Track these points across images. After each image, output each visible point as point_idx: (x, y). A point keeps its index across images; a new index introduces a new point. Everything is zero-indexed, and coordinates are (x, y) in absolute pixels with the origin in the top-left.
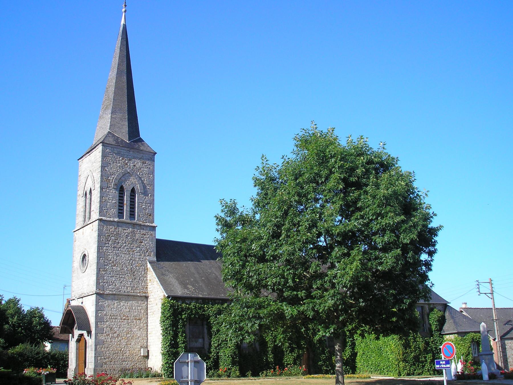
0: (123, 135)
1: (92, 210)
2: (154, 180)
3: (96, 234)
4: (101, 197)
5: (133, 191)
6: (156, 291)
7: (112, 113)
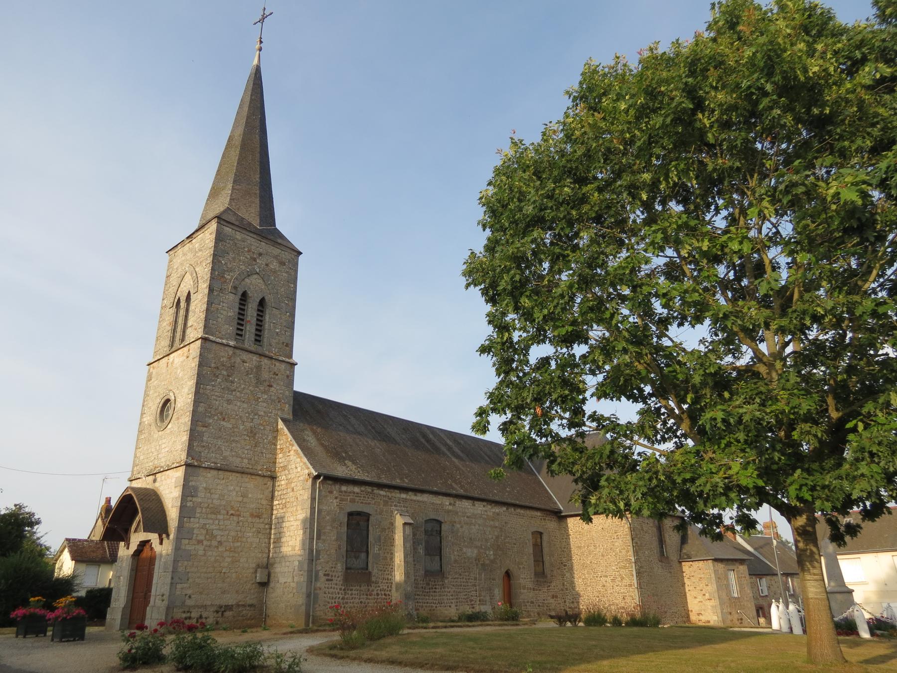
0: (252, 216)
1: (190, 323)
2: (295, 292)
3: (194, 364)
4: (210, 303)
5: (262, 303)
6: (293, 466)
7: (235, 182)
